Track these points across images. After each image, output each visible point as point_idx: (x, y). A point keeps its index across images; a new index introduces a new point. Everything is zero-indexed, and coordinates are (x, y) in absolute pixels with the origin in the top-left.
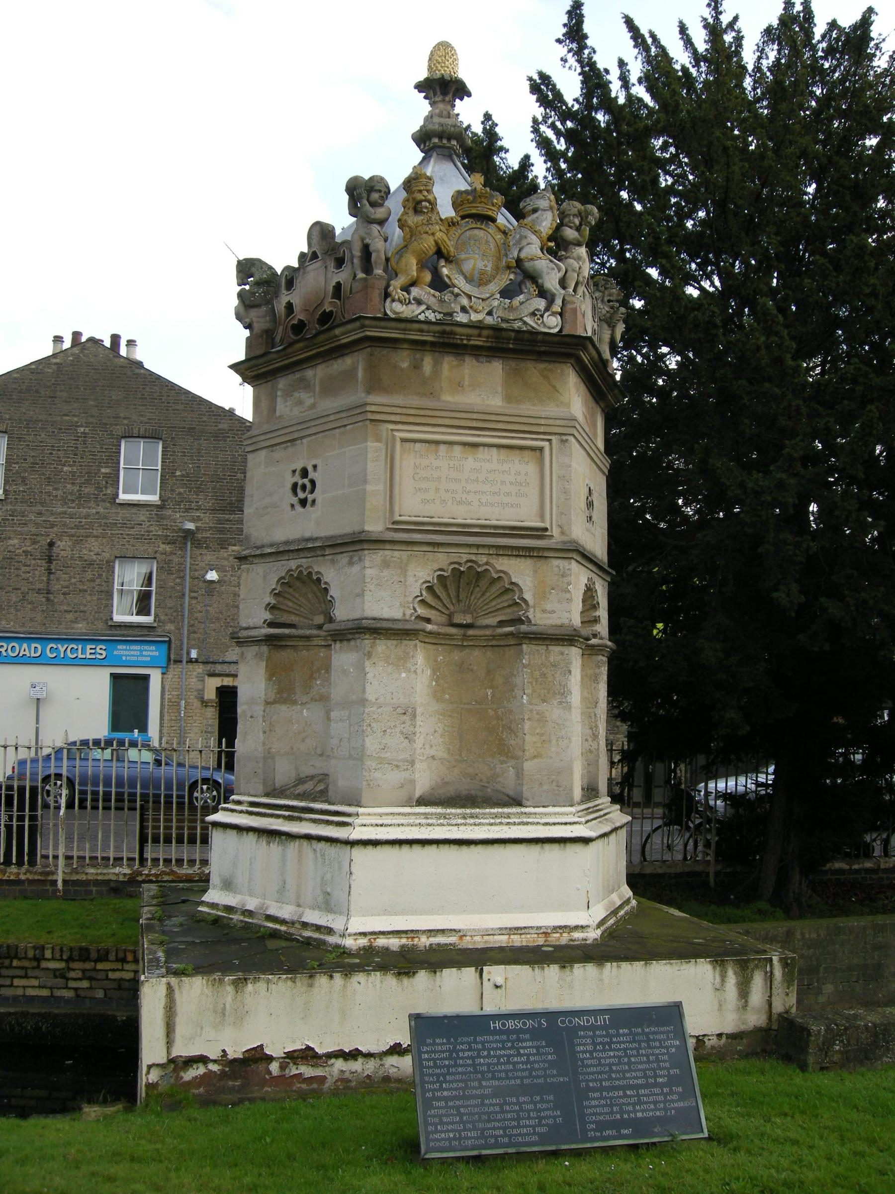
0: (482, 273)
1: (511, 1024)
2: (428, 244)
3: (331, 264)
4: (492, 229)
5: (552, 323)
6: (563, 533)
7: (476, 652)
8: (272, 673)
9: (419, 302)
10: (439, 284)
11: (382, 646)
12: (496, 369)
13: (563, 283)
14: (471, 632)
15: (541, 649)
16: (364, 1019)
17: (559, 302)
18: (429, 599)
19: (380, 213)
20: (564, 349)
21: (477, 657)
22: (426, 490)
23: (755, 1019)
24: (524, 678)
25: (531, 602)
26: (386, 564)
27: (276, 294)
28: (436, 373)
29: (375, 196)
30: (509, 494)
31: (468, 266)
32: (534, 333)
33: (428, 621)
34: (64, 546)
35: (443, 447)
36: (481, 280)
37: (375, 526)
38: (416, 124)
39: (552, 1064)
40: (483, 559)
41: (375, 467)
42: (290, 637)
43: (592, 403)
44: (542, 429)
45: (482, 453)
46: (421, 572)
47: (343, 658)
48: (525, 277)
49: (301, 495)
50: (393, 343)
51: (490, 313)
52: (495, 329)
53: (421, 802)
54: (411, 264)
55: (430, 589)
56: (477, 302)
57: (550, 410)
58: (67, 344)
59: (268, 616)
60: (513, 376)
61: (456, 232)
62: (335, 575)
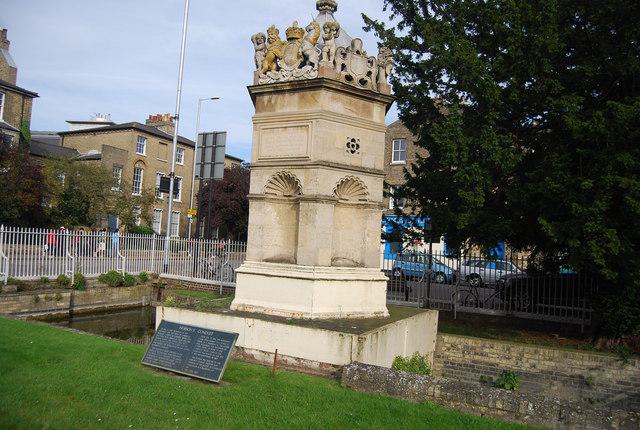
2: (271, 55)
5: (314, 75)
12: (296, 96)
48: (305, 60)
53: (267, 261)
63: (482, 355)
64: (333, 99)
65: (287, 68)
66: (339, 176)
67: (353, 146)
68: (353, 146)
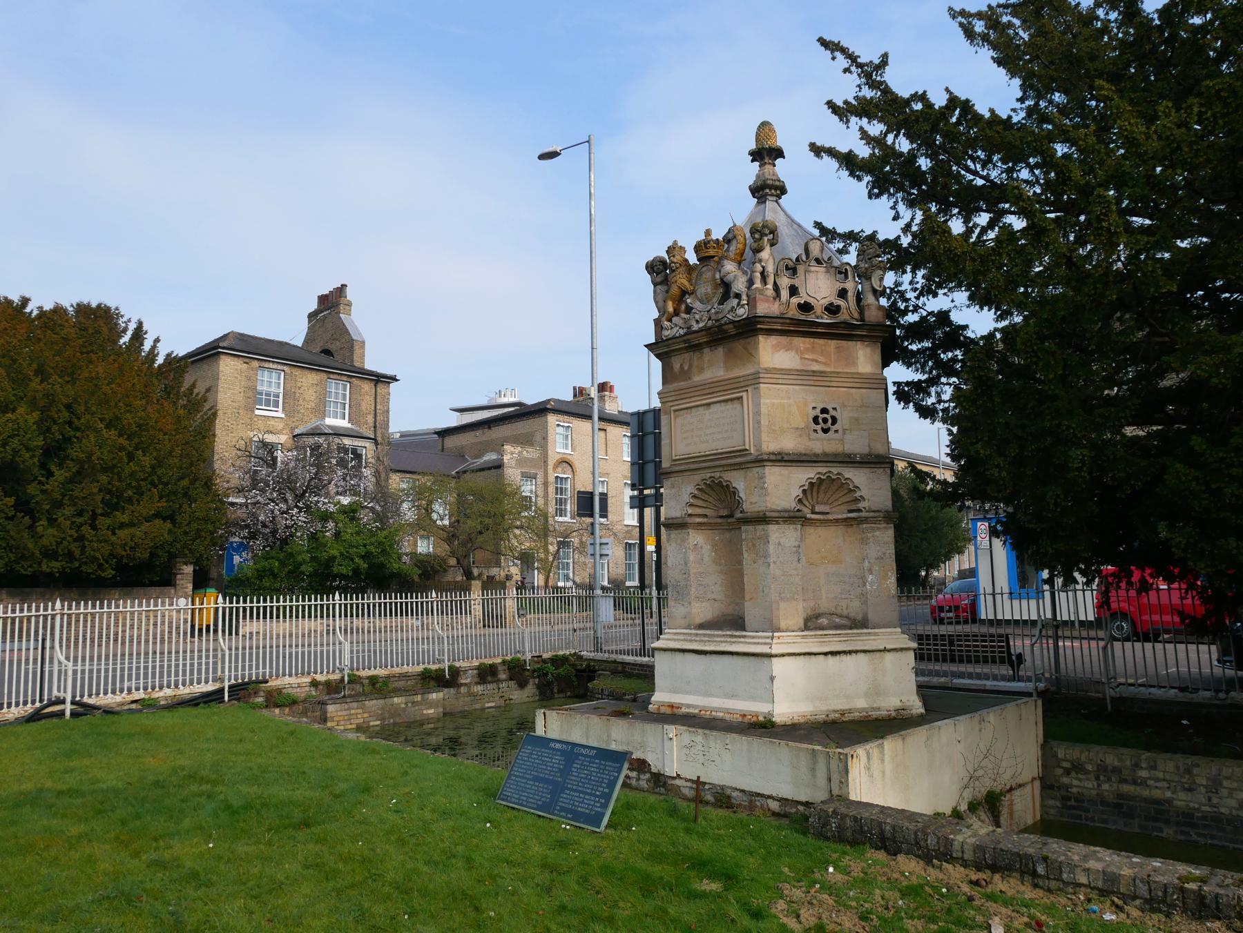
1: (558, 746)
12: (720, 352)
15: (750, 528)
26: (673, 486)
33: (706, 516)
40: (718, 475)
45: (714, 408)
57: (748, 370)
63: (1135, 783)
64: (776, 348)
66: (803, 475)
68: (825, 420)
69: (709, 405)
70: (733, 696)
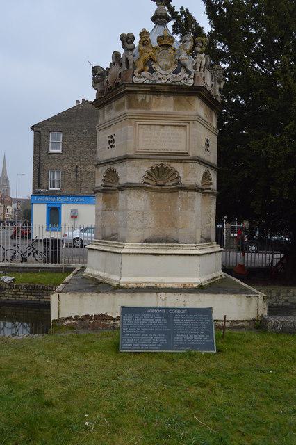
0: (166, 66)
1: (153, 311)
2: (146, 56)
3: (118, 65)
4: (170, 50)
5: (190, 82)
6: (193, 154)
7: (165, 194)
8: (105, 201)
9: (144, 77)
10: (152, 70)
11: (133, 192)
12: (171, 99)
13: (195, 68)
14: (163, 187)
16: (110, 305)
17: (193, 74)
18: (150, 177)
19: (131, 46)
20: (196, 91)
21: (166, 196)
22: (147, 141)
23: (252, 316)
24: (179, 202)
25: (182, 177)
27: (104, 78)
28: (150, 102)
29: (129, 40)
30: (174, 142)
31: (161, 64)
32: (184, 85)
33: (149, 184)
34: (81, 168)
35: (153, 126)
36: (166, 68)
37: (131, 153)
38: (152, 14)
39: (165, 325)
41: (131, 134)
42: (109, 190)
43: (209, 110)
44: (186, 119)
46: (145, 168)
47: (121, 195)
48: (181, 65)
49: (111, 144)
50: (135, 92)
51: (169, 79)
52: (170, 85)
53: (146, 241)
54: (141, 65)
55: (148, 173)
56: (164, 76)
57: (190, 112)
58: (81, 102)
59: (103, 183)
60: (177, 101)
61: (157, 52)
62: (119, 169)
65: (161, 71)
66: (202, 169)
67: (207, 145)
69: (163, 126)
70: (174, 276)
